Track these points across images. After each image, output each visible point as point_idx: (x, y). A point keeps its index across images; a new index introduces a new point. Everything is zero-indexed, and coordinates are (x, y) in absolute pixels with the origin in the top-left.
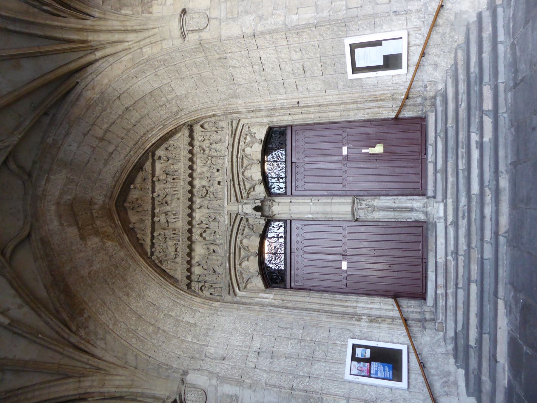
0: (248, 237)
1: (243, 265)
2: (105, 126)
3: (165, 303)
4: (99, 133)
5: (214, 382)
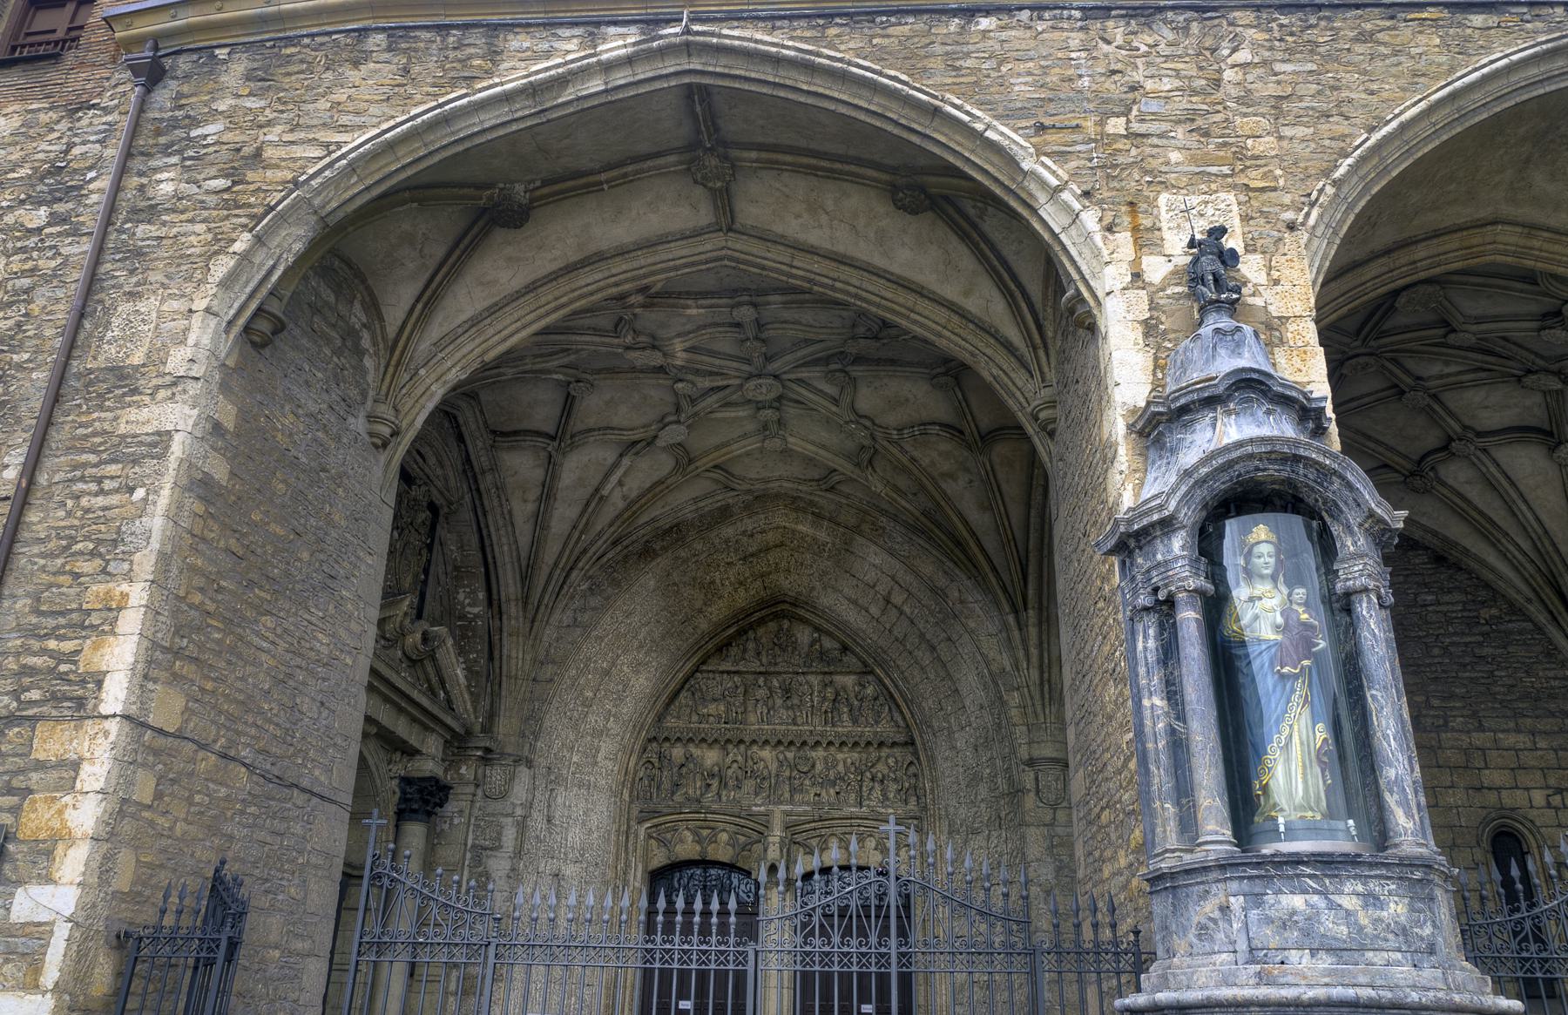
0: (732, 843)
1: (687, 833)
2: (907, 609)
3: (627, 709)
4: (898, 598)
5: (519, 811)
